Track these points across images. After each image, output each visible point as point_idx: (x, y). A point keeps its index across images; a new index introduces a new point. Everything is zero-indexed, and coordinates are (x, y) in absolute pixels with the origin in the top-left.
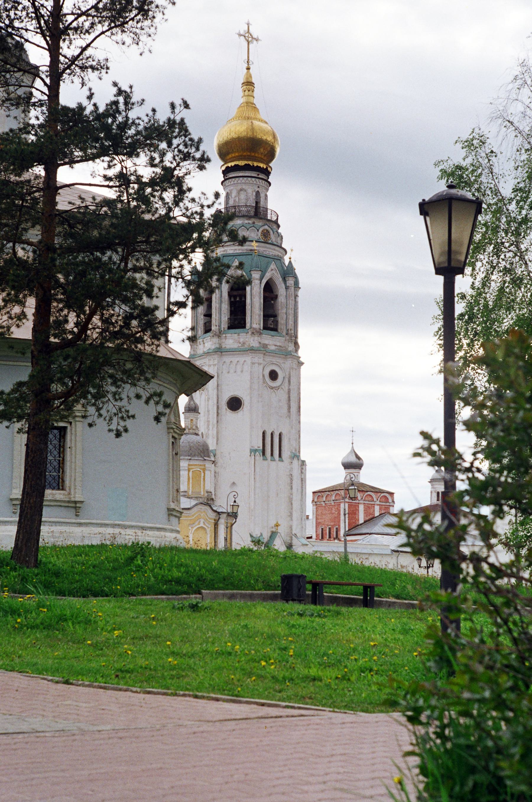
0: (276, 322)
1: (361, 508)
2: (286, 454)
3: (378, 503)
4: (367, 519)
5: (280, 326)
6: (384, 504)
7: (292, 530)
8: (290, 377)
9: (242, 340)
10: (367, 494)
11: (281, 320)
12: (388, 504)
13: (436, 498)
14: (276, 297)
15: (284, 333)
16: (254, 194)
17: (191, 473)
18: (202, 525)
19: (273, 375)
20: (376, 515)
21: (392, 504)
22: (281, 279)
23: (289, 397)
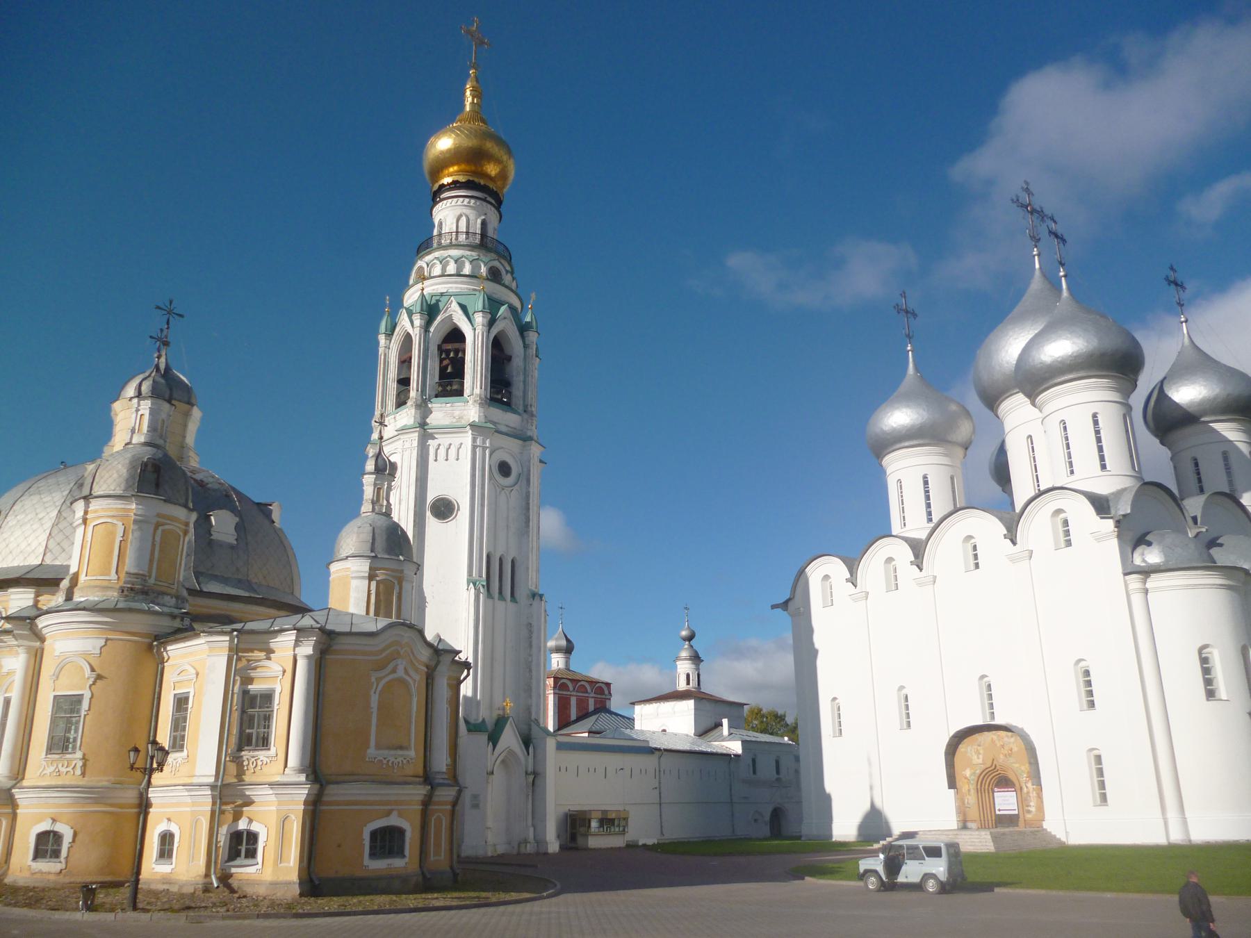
0: (509, 395)
1: (573, 701)
2: (522, 593)
3: (592, 695)
4: (580, 714)
5: (514, 400)
6: (599, 696)
7: (530, 713)
8: (529, 474)
9: (457, 413)
10: (579, 684)
11: (517, 391)
12: (604, 697)
13: (685, 682)
14: (509, 359)
15: (521, 409)
16: (479, 221)
17: (374, 584)
18: (400, 673)
19: (504, 469)
20: (590, 710)
21: (608, 697)
22: (518, 333)
23: (528, 504)
